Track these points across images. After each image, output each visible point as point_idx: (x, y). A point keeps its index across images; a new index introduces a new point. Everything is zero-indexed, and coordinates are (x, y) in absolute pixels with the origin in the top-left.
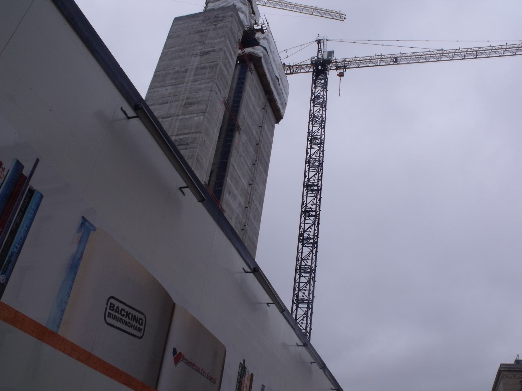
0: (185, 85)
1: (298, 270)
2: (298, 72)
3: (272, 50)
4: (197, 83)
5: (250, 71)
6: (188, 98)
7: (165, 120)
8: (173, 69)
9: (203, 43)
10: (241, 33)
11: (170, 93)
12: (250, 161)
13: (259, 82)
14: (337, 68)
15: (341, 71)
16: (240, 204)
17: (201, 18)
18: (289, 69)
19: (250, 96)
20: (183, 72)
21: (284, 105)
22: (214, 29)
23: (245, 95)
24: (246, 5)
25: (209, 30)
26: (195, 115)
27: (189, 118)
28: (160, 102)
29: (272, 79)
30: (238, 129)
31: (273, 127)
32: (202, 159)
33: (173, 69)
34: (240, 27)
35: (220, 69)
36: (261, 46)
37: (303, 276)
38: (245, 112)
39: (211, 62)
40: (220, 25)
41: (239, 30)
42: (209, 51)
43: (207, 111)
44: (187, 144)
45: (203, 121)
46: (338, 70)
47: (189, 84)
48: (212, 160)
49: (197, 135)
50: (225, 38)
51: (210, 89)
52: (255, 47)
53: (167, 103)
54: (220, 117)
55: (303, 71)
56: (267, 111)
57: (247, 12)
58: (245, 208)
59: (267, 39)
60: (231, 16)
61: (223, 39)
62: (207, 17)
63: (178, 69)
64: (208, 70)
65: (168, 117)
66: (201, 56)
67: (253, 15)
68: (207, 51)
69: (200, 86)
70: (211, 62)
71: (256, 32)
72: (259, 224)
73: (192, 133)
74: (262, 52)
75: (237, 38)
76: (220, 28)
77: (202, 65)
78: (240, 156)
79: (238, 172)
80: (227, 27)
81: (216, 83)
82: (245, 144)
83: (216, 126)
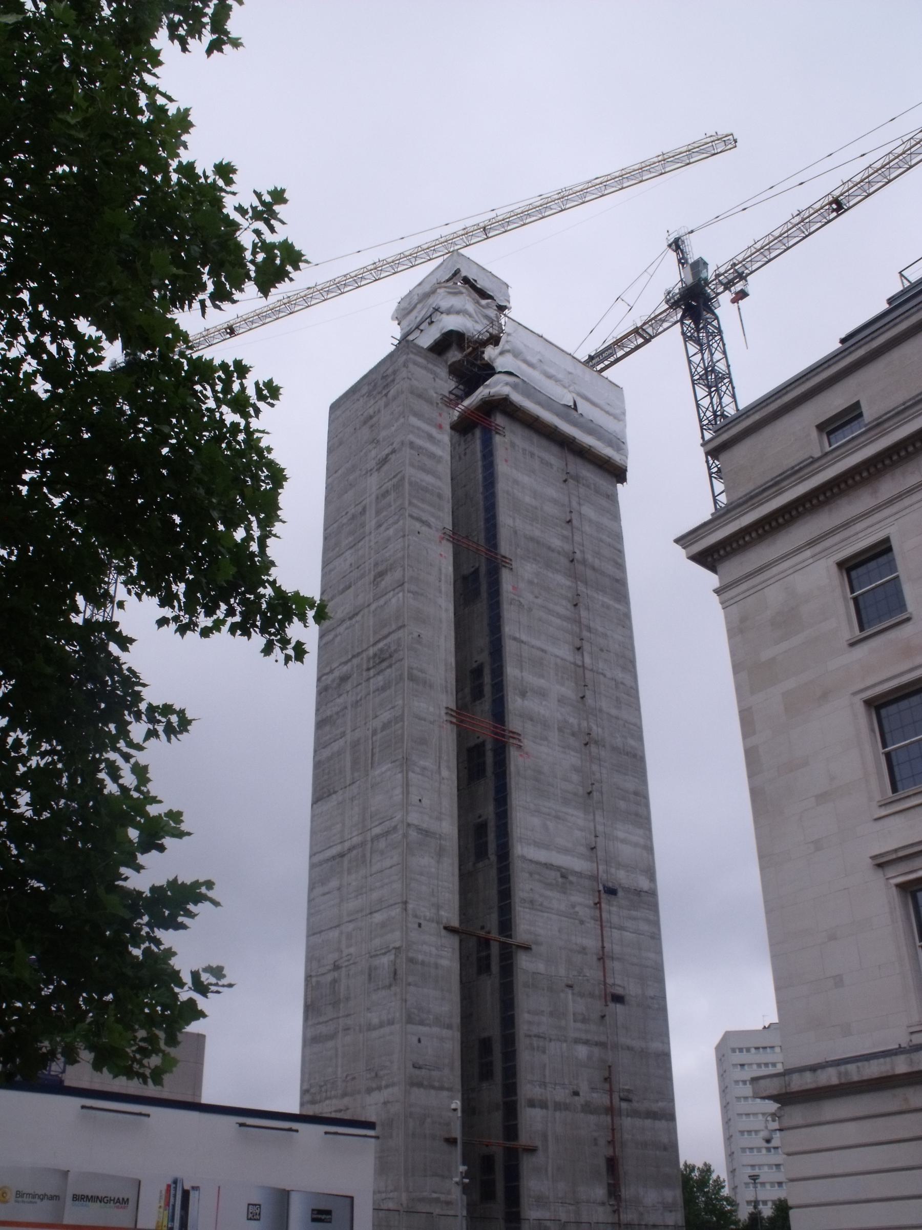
0: (367, 539)
2: (659, 331)
3: (534, 360)
4: (383, 528)
5: (497, 433)
6: (376, 565)
7: (354, 620)
8: (347, 513)
9: (375, 441)
10: (442, 379)
11: (351, 565)
12: (564, 602)
13: (535, 438)
14: (728, 286)
15: (739, 287)
16: (562, 701)
17: (365, 390)
18: (638, 337)
19: (516, 482)
20: (361, 513)
21: (619, 444)
22: (386, 405)
23: (502, 486)
24: (461, 293)
25: (379, 411)
26: (392, 593)
27: (385, 603)
28: (342, 587)
29: (558, 415)
30: (505, 562)
31: (613, 499)
32: (422, 671)
33: (347, 513)
34: (435, 368)
35: (411, 484)
36: (500, 372)
38: (514, 519)
39: (394, 477)
40: (392, 392)
41: (436, 376)
42: (387, 455)
43: (406, 580)
44: (391, 656)
45: (404, 602)
46: (732, 289)
47: (373, 535)
48: (452, 660)
49: (400, 634)
50: (404, 417)
51: (401, 534)
52: (487, 383)
53: (350, 587)
54: (444, 571)
55: (666, 325)
56: (577, 478)
57: (470, 307)
58: (580, 700)
59: (508, 351)
60: (405, 365)
61: (402, 420)
62: (373, 384)
63: (353, 511)
64: (392, 496)
65: (357, 614)
66: (378, 470)
67: (484, 302)
68: (384, 457)
69: (387, 532)
70: (394, 477)
71: (483, 349)
72: (638, 709)
73: (393, 632)
74: (507, 384)
75: (435, 395)
76: (394, 398)
77: (383, 487)
78: (530, 610)
79: (534, 642)
80: (402, 392)
81: (411, 516)
82: (536, 581)
83: (440, 592)
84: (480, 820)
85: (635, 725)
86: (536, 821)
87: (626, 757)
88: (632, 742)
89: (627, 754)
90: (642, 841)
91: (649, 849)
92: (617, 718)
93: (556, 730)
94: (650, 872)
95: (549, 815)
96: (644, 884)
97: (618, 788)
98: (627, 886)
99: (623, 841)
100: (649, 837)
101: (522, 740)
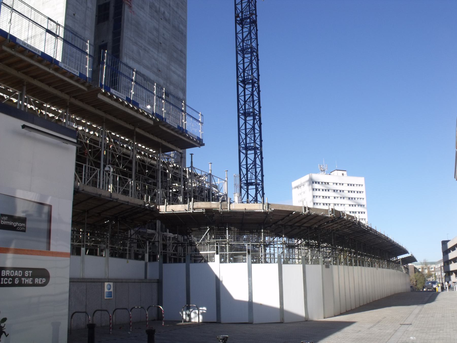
1: (239, 52)
37: (246, 58)
84: (104, 43)
85: (184, 19)
86: (135, 48)
87: (179, 33)
88: (181, 26)
89: (179, 31)
90: (181, 75)
91: (185, 80)
92: (176, 12)
93: (148, 7)
94: (184, 91)
95: (141, 47)
96: (181, 95)
97: (174, 46)
98: (173, 94)
99: (174, 72)
100: (185, 74)
101: (132, 4)
